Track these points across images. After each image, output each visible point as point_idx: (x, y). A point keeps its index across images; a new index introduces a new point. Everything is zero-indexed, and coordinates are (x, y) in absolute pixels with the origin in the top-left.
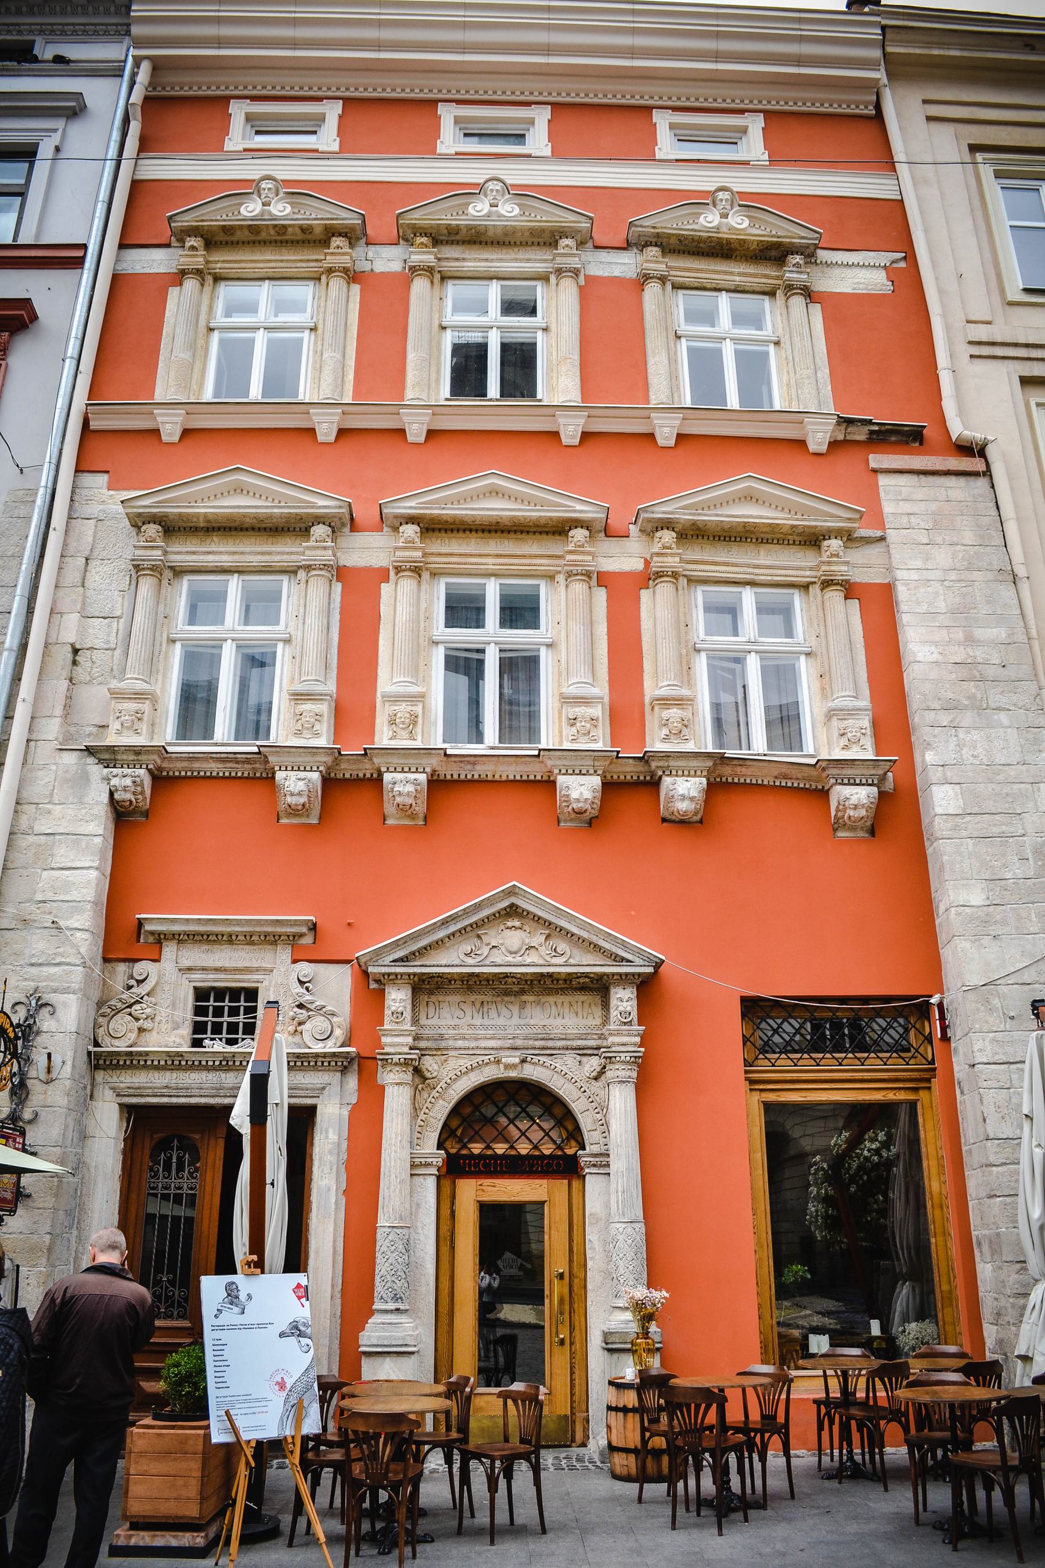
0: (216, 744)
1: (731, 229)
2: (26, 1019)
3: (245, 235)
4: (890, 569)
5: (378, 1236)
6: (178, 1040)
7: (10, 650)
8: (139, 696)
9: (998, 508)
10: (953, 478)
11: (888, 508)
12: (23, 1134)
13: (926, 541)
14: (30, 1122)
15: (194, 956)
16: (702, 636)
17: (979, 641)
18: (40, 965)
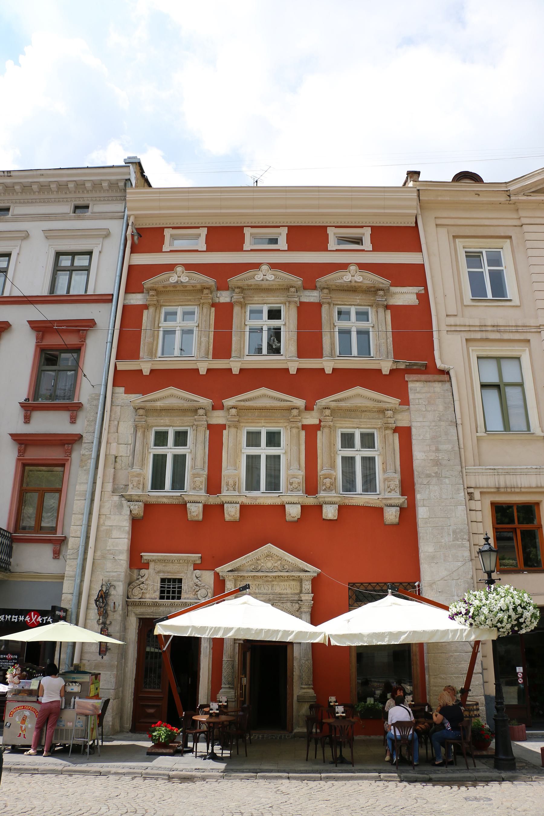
0: (166, 492)
1: (356, 282)
2: (106, 591)
3: (172, 289)
4: (410, 421)
5: (223, 663)
6: (156, 597)
7: (94, 459)
8: (139, 475)
9: (453, 395)
10: (437, 383)
11: (411, 396)
12: (107, 629)
13: (424, 410)
14: (109, 625)
15: (159, 567)
16: (340, 448)
17: (441, 450)
18: (110, 572)
